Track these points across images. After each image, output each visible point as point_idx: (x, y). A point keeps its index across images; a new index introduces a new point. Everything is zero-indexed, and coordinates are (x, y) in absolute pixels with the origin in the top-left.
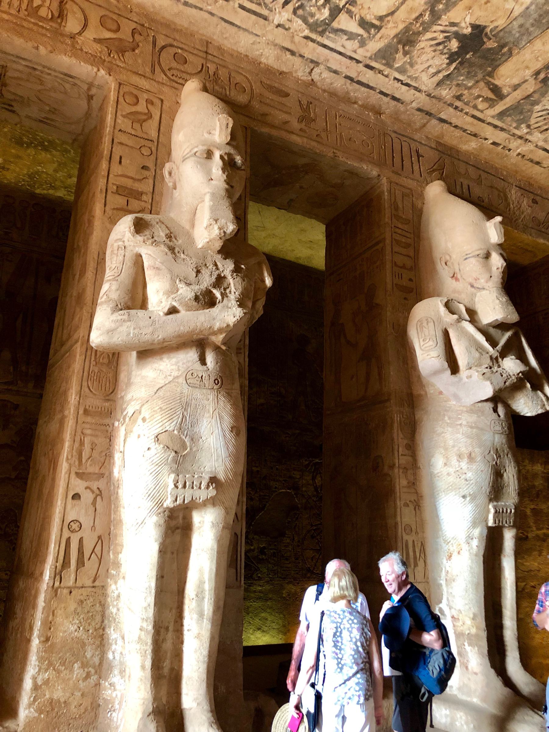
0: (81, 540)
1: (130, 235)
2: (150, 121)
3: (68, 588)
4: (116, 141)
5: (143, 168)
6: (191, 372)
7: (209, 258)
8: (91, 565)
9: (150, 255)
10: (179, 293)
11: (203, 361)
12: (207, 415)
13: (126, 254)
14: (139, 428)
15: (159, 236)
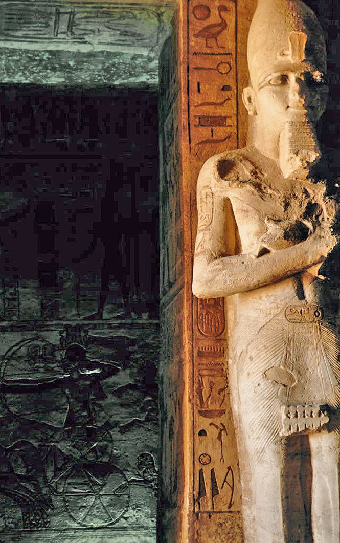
0: (212, 471)
1: (215, 181)
2: (225, 31)
3: (207, 512)
4: (191, 66)
5: (223, 89)
6: (290, 308)
7: (298, 187)
8: (224, 492)
9: (237, 198)
10: (268, 233)
11: (301, 295)
12: (311, 347)
13: (215, 200)
14: (249, 366)
15: (244, 175)
